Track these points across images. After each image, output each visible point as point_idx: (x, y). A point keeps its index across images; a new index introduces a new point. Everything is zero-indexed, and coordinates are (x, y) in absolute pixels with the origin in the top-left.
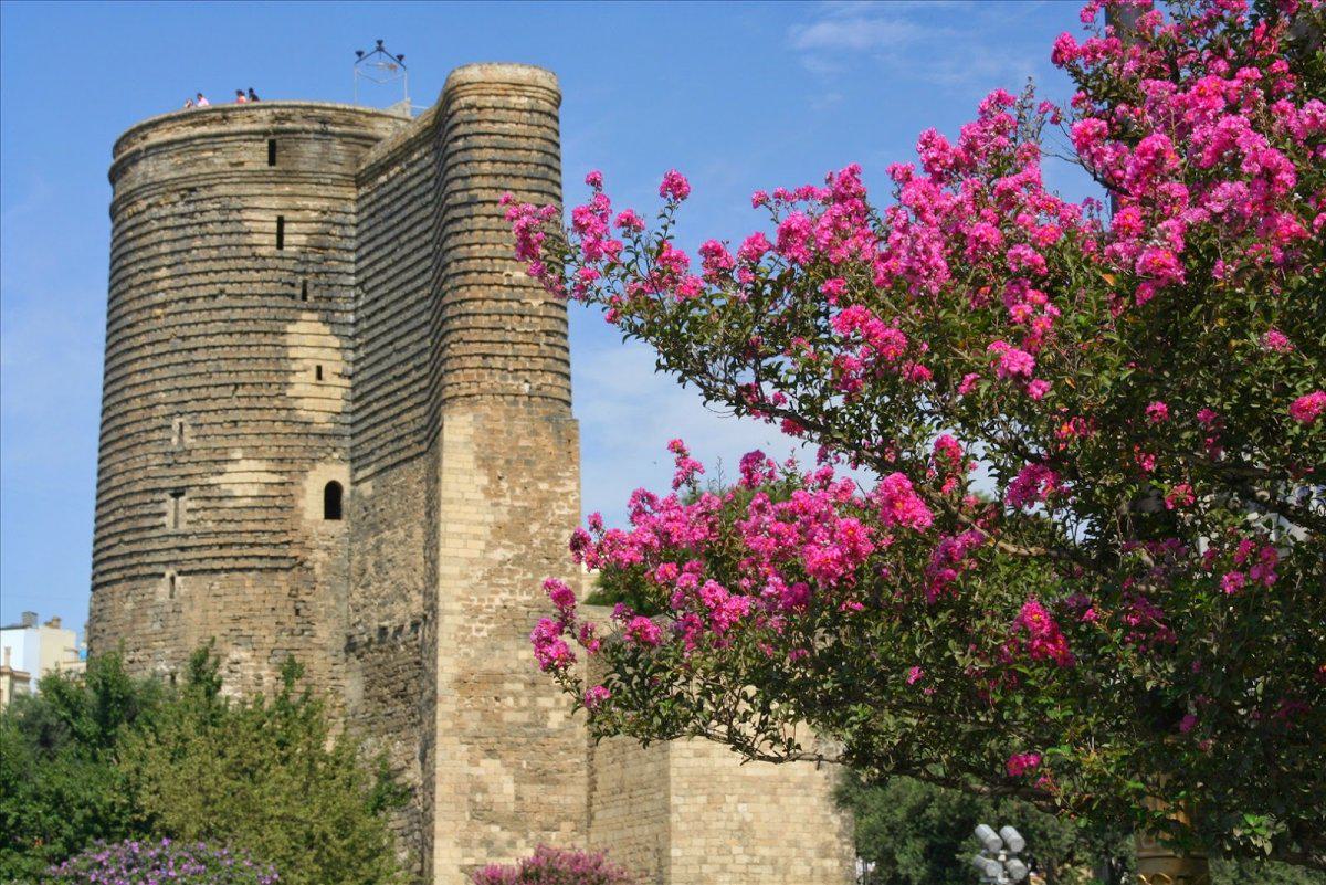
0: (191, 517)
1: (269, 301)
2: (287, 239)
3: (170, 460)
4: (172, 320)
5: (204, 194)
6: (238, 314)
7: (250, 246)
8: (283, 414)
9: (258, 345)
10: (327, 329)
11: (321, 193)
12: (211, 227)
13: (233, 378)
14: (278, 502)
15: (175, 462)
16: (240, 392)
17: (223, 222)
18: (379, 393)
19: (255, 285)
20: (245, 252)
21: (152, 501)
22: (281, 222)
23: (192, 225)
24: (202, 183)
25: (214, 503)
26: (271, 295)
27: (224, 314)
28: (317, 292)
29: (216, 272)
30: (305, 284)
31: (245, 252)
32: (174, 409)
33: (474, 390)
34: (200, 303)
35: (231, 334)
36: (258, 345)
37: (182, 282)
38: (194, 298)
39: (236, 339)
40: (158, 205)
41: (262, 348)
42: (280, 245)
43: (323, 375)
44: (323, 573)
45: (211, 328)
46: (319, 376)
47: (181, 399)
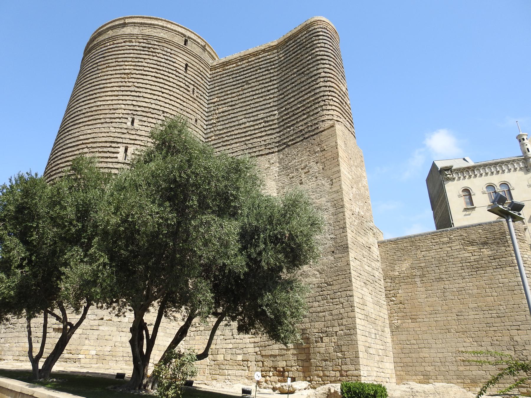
1: (181, 89)
3: (125, 131)
15: (128, 132)
17: (164, 55)
18: (229, 134)
20: (174, 69)
22: (187, 65)
26: (181, 87)
27: (161, 85)
30: (194, 89)
31: (174, 69)
33: (339, 119)
35: (163, 93)
45: (154, 88)
47: (135, 109)
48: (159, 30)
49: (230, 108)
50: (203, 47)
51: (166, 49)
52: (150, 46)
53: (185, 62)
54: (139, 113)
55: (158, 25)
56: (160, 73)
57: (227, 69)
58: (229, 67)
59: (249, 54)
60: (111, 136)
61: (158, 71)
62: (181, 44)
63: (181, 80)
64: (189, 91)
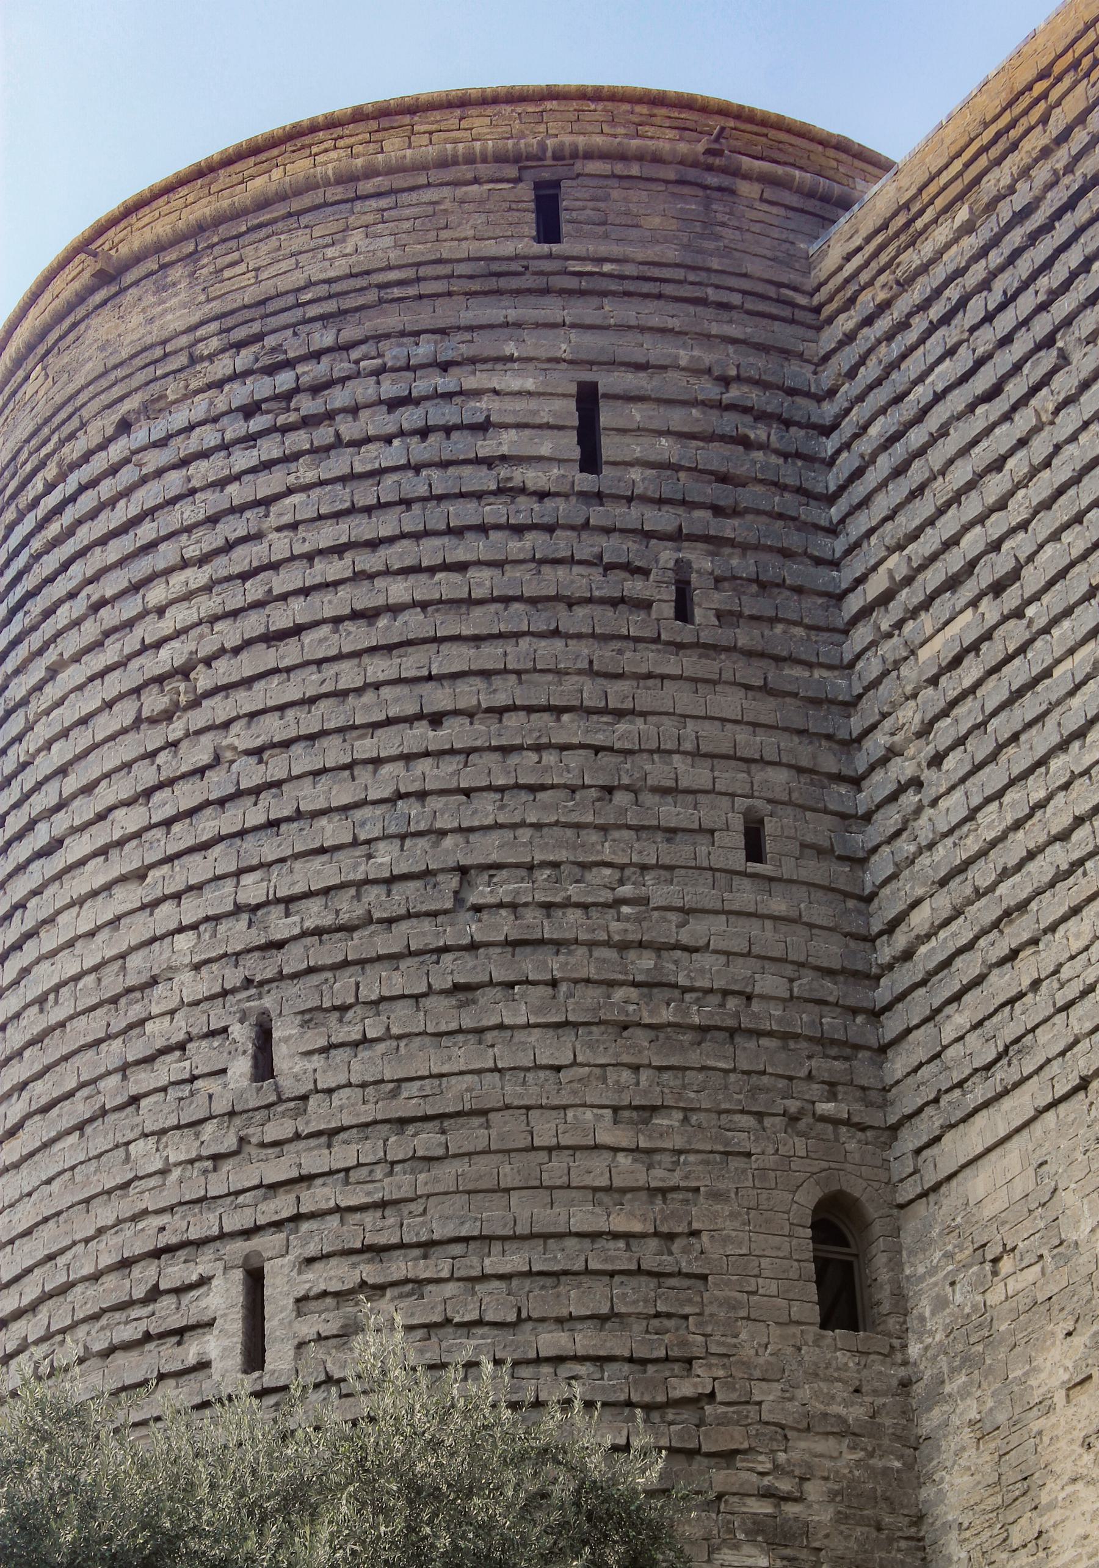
0: (308, 1328)
2: (610, 447)
4: (219, 709)
5: (324, 338)
6: (456, 658)
7: (488, 462)
8: (644, 963)
9: (538, 748)
10: (765, 709)
11: (715, 329)
12: (348, 429)
13: (452, 850)
14: (650, 1254)
15: (242, 1140)
16: (481, 893)
17: (394, 404)
18: (1021, 842)
19: (512, 572)
20: (483, 479)
21: (154, 1294)
23: (285, 429)
24: (312, 311)
25: (399, 1267)
26: (571, 603)
27: (411, 664)
28: (720, 599)
29: (373, 544)
30: (682, 567)
31: (483, 479)
32: (233, 977)
34: (315, 644)
35: (436, 720)
36: (538, 748)
37: (254, 590)
38: (297, 630)
39: (454, 733)
40: (152, 409)
41: (550, 758)
42: (590, 461)
43: (769, 845)
44: (841, 1518)
45: (365, 708)
46: (755, 850)
48: (324, 226)
49: (992, 611)
50: (709, 168)
51: (393, 353)
52: (285, 380)
53: (566, 382)
54: (293, 959)
55: (310, 186)
56: (387, 572)
57: (924, 269)
58: (927, 249)
59: (1042, 76)
60: (145, 1213)
61: (369, 561)
62: (508, 248)
63: (562, 543)
64: (645, 605)
